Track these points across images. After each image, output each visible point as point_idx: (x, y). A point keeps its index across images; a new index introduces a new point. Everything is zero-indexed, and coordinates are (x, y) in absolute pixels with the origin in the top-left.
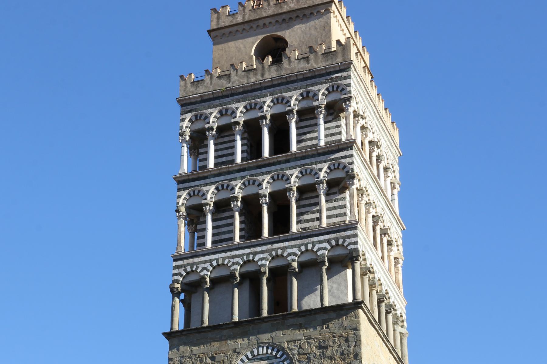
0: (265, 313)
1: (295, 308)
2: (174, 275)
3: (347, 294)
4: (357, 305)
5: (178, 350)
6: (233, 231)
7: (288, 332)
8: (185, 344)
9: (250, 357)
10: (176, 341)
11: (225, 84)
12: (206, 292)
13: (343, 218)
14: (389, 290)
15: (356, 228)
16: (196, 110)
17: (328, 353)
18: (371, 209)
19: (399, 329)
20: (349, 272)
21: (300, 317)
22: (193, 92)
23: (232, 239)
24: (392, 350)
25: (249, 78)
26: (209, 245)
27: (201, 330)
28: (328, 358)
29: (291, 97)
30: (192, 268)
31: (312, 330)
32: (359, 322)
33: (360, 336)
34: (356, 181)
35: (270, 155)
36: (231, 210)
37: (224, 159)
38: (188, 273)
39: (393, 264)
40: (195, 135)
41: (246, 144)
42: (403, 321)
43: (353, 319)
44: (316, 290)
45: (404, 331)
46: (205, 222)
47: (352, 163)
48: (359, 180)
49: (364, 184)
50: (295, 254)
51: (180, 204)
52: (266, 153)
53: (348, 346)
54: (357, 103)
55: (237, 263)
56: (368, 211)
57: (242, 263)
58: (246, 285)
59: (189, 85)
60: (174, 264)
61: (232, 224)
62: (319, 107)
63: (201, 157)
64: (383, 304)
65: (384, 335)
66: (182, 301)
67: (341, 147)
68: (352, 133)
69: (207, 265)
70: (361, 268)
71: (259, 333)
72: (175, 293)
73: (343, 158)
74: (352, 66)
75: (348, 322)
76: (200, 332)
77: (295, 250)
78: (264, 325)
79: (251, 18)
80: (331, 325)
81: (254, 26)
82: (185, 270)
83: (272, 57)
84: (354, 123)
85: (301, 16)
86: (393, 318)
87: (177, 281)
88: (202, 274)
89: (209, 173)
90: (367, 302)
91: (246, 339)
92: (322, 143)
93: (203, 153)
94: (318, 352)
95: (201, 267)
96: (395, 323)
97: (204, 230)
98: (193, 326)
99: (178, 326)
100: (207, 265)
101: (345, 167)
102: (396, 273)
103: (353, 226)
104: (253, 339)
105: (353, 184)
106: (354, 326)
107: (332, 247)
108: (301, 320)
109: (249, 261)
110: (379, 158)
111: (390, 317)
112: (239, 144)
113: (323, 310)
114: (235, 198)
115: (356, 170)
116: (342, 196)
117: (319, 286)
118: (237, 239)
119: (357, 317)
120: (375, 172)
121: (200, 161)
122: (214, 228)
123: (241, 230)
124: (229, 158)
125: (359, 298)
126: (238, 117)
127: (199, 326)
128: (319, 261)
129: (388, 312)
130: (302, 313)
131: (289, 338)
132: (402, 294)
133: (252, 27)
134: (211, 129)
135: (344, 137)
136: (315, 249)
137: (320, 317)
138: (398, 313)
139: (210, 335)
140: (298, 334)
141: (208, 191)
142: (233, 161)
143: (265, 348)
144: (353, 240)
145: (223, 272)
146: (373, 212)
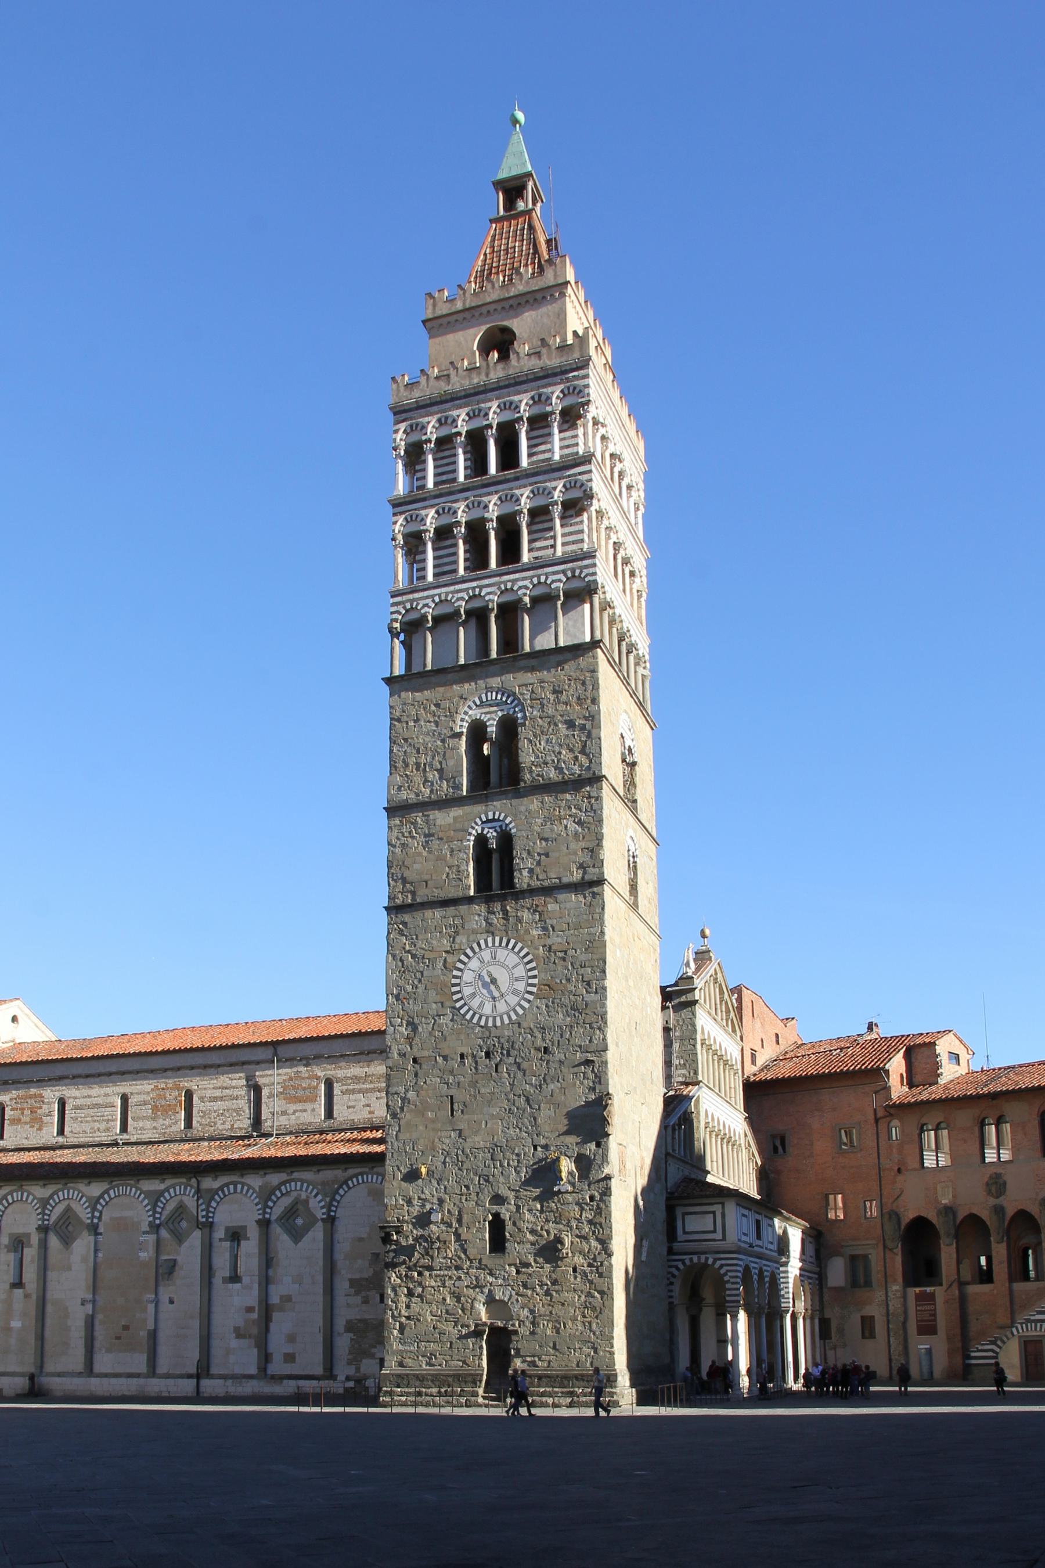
0: (494, 655)
1: (527, 649)
2: (392, 613)
3: (584, 632)
4: (595, 644)
5: (399, 696)
6: (456, 562)
7: (519, 675)
8: (407, 690)
9: (478, 703)
10: (396, 687)
11: (443, 387)
12: (428, 632)
13: (579, 546)
14: (630, 628)
15: (594, 557)
16: (411, 419)
17: (563, 698)
18: (612, 534)
19: (641, 671)
20: (587, 607)
21: (533, 658)
22: (407, 396)
23: (455, 571)
24: (633, 694)
25: (471, 378)
26: (430, 578)
27: (424, 674)
28: (563, 703)
29: (521, 401)
30: (411, 605)
31: (545, 673)
32: (597, 663)
33: (598, 679)
34: (595, 501)
35: (497, 472)
36: (454, 537)
37: (444, 478)
38: (407, 611)
39: (636, 597)
40: (410, 449)
41: (469, 459)
42: (645, 662)
43: (591, 660)
44: (550, 627)
45: (646, 672)
46: (424, 552)
47: (591, 480)
48: (599, 500)
49: (604, 505)
50: (526, 588)
51: (396, 531)
52: (493, 469)
53: (585, 690)
54: (597, 408)
55: (462, 599)
56: (608, 538)
57: (467, 598)
58: (473, 623)
59: (402, 389)
60: (392, 601)
61: (455, 554)
62: (552, 413)
63: (419, 475)
64: (624, 643)
65: (624, 678)
66: (401, 642)
67: (578, 461)
68: (590, 444)
69: (429, 601)
70: (600, 603)
71: (487, 677)
72: (394, 634)
73: (580, 474)
74: (591, 363)
75: (585, 663)
76: (422, 677)
77: (527, 583)
78: (492, 668)
79: (473, 304)
80: (566, 667)
81: (477, 314)
82: (404, 608)
83: (499, 353)
84: (593, 432)
85: (531, 301)
86: (635, 658)
87: (396, 620)
88: (423, 611)
89: (428, 495)
90: (606, 641)
91: (473, 684)
92: (557, 457)
93: (420, 471)
94: (552, 697)
95: (421, 603)
96: (637, 664)
97: (424, 560)
98: (414, 671)
99: (399, 670)
100: (429, 601)
101: (582, 485)
102: (639, 607)
103: (591, 555)
104: (481, 683)
105: (591, 505)
106: (592, 667)
107: (568, 579)
108: (533, 662)
109: (475, 596)
110: (621, 474)
111: (631, 657)
112: (461, 458)
113: (558, 650)
114: (458, 524)
115: (595, 489)
116: (578, 519)
117: (553, 624)
118: (461, 571)
119: (595, 657)
120: (617, 491)
121: (417, 479)
122: (435, 558)
123: (466, 560)
124: (451, 476)
125: (598, 636)
126: (459, 426)
127: (422, 670)
128: (553, 594)
129: (629, 652)
130: (535, 654)
131: (520, 683)
132: (645, 632)
133: (474, 316)
134: (430, 441)
135: (581, 450)
136: (548, 582)
137: (554, 658)
138: (641, 653)
139: (433, 679)
140: (530, 677)
141: (427, 516)
142: (454, 480)
143: (494, 693)
144: (591, 570)
145: (447, 609)
146: (614, 538)
